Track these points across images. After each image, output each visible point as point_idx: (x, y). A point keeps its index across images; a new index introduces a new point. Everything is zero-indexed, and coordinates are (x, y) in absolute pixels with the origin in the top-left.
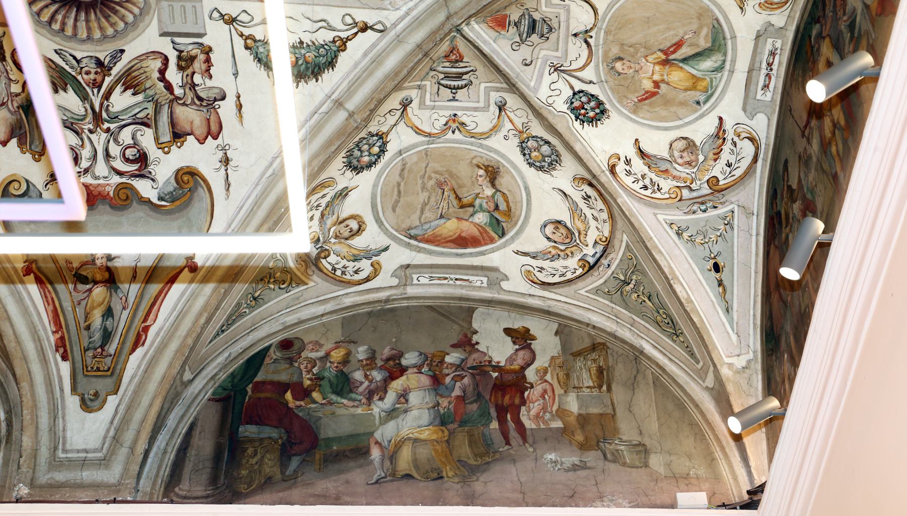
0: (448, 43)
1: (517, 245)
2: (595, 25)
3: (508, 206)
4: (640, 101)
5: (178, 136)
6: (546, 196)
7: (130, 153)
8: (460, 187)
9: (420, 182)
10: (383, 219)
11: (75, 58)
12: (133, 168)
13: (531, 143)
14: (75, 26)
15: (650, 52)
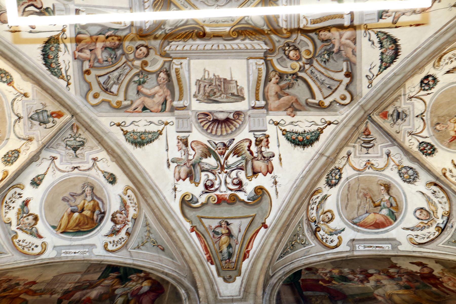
0: (365, 125)
1: (403, 225)
2: (425, 110)
3: (397, 204)
4: (451, 141)
5: (255, 173)
6: (414, 196)
7: (235, 181)
8: (374, 196)
9: (356, 194)
10: (342, 214)
11: (215, 143)
12: (236, 187)
13: (404, 171)
14: (216, 131)
15: (451, 118)
